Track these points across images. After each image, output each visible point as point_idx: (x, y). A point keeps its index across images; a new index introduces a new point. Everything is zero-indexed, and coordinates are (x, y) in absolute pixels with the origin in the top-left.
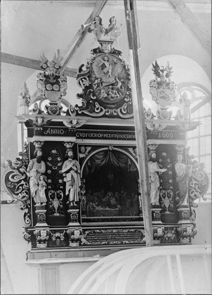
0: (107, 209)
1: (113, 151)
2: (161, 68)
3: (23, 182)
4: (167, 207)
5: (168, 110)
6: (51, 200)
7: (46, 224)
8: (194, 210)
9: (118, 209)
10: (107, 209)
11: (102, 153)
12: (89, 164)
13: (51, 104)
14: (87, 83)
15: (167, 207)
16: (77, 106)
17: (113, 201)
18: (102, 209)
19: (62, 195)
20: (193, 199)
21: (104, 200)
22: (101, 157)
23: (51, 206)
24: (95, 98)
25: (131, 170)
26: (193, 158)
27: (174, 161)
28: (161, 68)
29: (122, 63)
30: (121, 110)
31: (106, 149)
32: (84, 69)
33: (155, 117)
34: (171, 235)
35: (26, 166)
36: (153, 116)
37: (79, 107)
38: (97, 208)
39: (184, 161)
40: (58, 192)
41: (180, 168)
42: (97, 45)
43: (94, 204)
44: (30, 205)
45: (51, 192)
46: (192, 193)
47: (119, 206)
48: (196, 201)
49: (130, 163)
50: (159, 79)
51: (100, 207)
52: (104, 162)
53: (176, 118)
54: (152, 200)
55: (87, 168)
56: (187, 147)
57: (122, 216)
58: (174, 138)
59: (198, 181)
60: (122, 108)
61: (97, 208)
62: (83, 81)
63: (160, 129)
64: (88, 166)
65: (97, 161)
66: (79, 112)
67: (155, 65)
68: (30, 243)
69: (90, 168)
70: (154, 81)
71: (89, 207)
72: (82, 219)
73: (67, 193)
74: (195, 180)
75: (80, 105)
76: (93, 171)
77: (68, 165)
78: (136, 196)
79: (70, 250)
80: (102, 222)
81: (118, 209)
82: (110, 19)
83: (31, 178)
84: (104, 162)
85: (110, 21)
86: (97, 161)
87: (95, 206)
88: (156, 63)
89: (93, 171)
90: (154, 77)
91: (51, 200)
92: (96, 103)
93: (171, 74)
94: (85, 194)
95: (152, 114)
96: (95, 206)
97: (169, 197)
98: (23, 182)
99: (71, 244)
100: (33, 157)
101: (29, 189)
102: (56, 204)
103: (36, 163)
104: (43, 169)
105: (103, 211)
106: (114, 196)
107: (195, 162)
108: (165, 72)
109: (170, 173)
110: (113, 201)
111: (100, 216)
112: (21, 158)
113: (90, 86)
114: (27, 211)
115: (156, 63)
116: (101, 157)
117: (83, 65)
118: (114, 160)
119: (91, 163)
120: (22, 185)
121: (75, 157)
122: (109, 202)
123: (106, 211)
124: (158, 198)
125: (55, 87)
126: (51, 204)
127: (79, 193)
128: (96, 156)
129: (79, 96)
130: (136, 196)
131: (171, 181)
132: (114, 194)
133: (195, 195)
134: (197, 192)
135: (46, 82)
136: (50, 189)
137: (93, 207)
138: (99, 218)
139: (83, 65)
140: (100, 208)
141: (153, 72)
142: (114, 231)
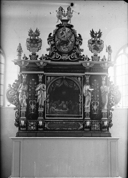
0: (61, 110)
1: (66, 79)
2: (95, 33)
3: (16, 96)
4: (95, 110)
5: (98, 56)
6: (93, 105)
7: (25, 118)
8: (111, 113)
10: (61, 110)
11: (59, 80)
12: (52, 86)
13: (32, 54)
14: (52, 42)
15: (95, 110)
16: (46, 55)
17: (65, 106)
18: (58, 110)
19: (99, 103)
20: (111, 106)
21: (60, 105)
22: (59, 82)
23: (92, 109)
24: (56, 50)
25: (76, 89)
26: (112, 83)
27: (101, 84)
28: (95, 33)
29: (73, 31)
30: (70, 57)
31: (61, 77)
32: (52, 35)
33: (90, 59)
34: (96, 126)
35: (18, 87)
36: (89, 59)
37: (47, 56)
38: (55, 110)
39: (106, 84)
40: (34, 101)
41: (104, 88)
42: (60, 22)
43: (54, 108)
44: (19, 107)
45: (93, 102)
46: (111, 102)
47: (68, 109)
48: (113, 107)
49: (75, 85)
50: (93, 39)
51: (57, 109)
52: (61, 85)
53: (103, 60)
54: (86, 106)
55: (51, 88)
56: (109, 76)
57: (73, 114)
58: (100, 72)
59: (115, 96)
60: (71, 55)
61: (55, 110)
62: (50, 42)
63: (91, 66)
64: (52, 87)
65: (57, 84)
66: (48, 57)
67: (92, 31)
68: (18, 127)
69: (53, 88)
70: (90, 40)
71: (51, 110)
73: (38, 102)
74: (113, 95)
75: (48, 54)
76: (54, 90)
77: (40, 86)
78: (78, 104)
79: (21, 132)
80: (74, 117)
82: (68, 8)
83: (20, 93)
84: (61, 85)
85: (68, 9)
86: (57, 84)
87: (54, 109)
88: (92, 30)
89: (54, 90)
90: (90, 38)
91: (93, 105)
92: (57, 53)
93: (101, 36)
94: (49, 102)
95: (88, 58)
96: (54, 109)
97: (97, 105)
98: (16, 96)
99: (104, 130)
100: (21, 82)
101: (18, 100)
102: (33, 107)
103: (22, 85)
104: (26, 88)
105: (59, 111)
106: (65, 103)
107: (113, 85)
108: (98, 35)
109: (98, 91)
110: (65, 106)
112: (16, 83)
113: (54, 44)
114: (17, 110)
115: (92, 30)
116: (59, 82)
117: (51, 34)
118: (66, 83)
119: (54, 86)
120: (15, 97)
121: (43, 82)
123: (61, 111)
124: (90, 104)
125: (36, 45)
126: (30, 107)
127: (45, 102)
128: (57, 81)
129: (48, 50)
130: (78, 104)
131: (98, 96)
132: (65, 102)
133: (112, 104)
134: (113, 102)
135: (31, 42)
136: (30, 100)
138: (56, 115)
139: (51, 34)
140: (57, 110)
141: (90, 35)
142: (64, 123)
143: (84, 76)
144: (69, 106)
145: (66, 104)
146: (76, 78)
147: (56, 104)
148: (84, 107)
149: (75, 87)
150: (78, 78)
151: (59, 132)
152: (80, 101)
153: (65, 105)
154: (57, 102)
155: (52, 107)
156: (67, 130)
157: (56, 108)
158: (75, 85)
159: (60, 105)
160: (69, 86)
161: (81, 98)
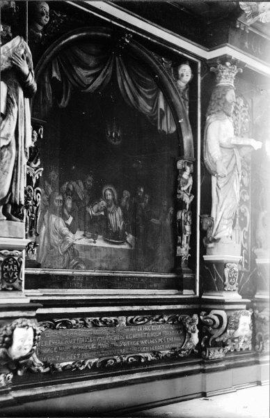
0: (100, 243)
9: (125, 246)
12: (55, 74)
17: (116, 219)
18: (84, 242)
21: (92, 211)
47: (130, 238)
51: (79, 234)
71: (48, 233)
72: (27, 275)
81: (125, 246)
87: (66, 231)
89: (64, 103)
105: (86, 248)
106: (118, 203)
111: (76, 267)
122: (105, 219)
123: (97, 249)
132: (120, 196)
137: (63, 236)
143: (213, 62)
144: (137, 222)
145: (123, 209)
146: (166, 63)
147: (76, 201)
148: (204, 233)
149: (163, 114)
150: (176, 66)
151: (99, 382)
152: (188, 200)
153: (119, 212)
154: (79, 187)
155: (54, 219)
156: (133, 364)
157: (72, 229)
158: (162, 105)
159: (92, 211)
160: (136, 99)
161: (191, 182)
